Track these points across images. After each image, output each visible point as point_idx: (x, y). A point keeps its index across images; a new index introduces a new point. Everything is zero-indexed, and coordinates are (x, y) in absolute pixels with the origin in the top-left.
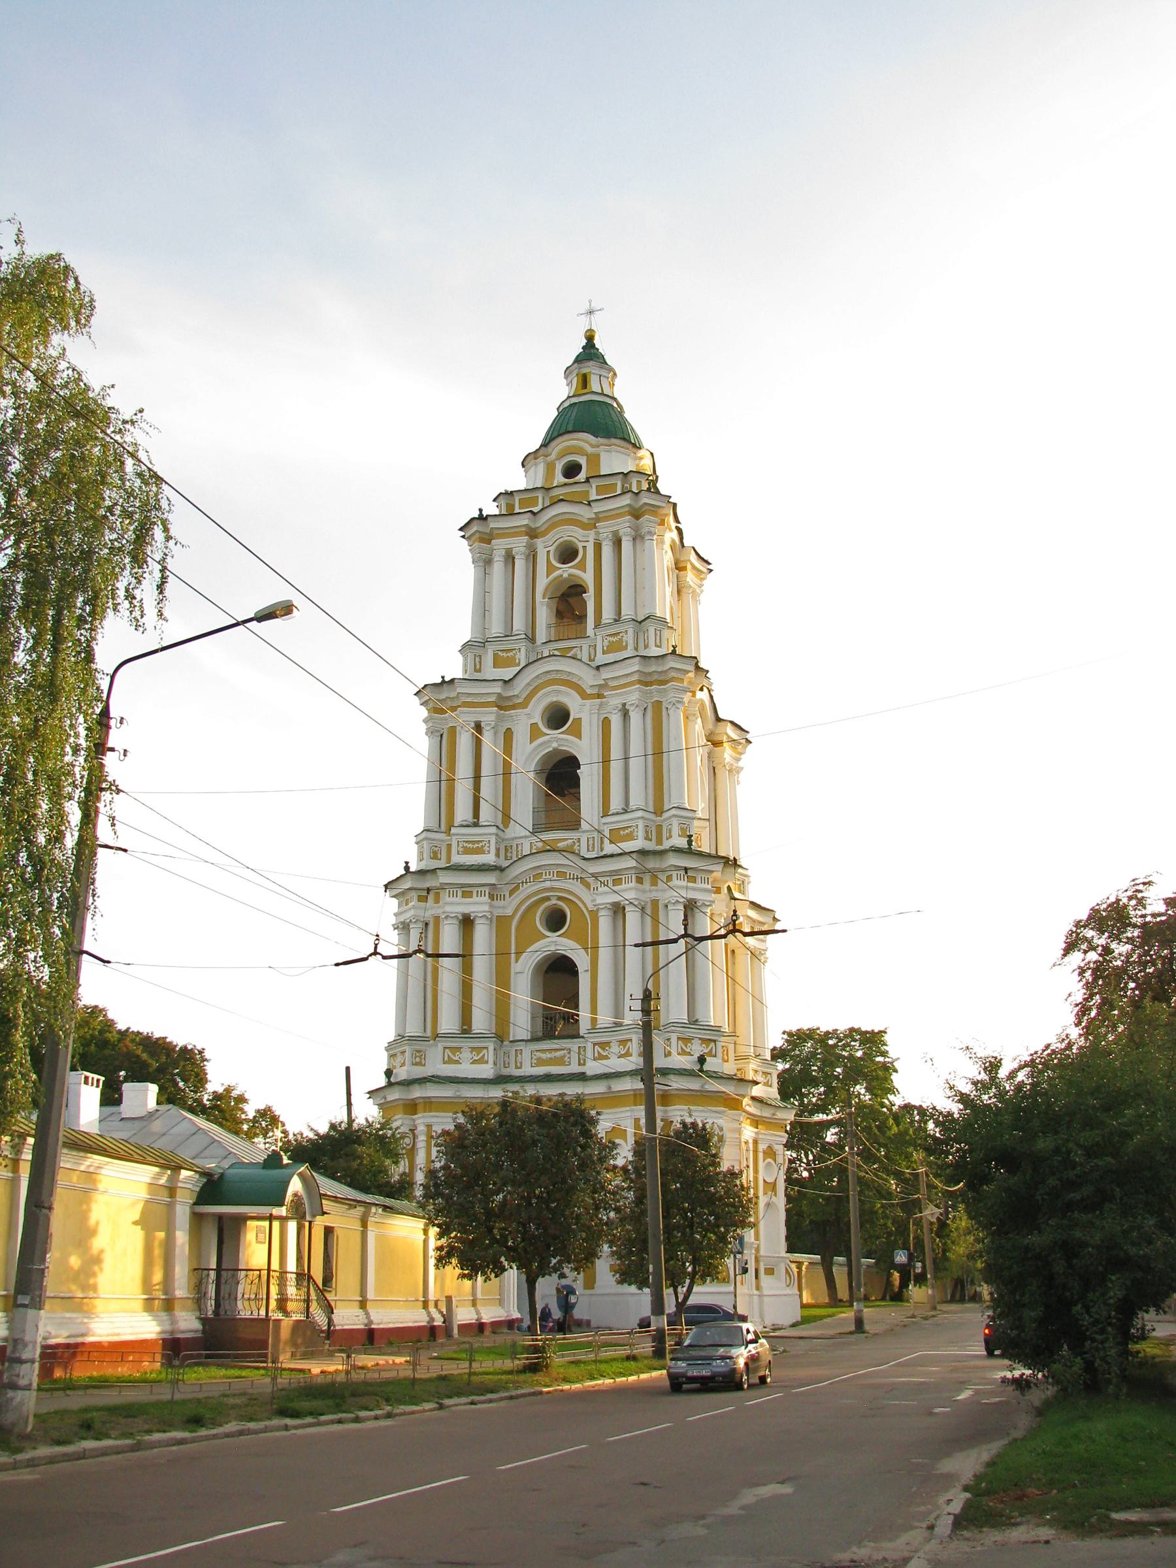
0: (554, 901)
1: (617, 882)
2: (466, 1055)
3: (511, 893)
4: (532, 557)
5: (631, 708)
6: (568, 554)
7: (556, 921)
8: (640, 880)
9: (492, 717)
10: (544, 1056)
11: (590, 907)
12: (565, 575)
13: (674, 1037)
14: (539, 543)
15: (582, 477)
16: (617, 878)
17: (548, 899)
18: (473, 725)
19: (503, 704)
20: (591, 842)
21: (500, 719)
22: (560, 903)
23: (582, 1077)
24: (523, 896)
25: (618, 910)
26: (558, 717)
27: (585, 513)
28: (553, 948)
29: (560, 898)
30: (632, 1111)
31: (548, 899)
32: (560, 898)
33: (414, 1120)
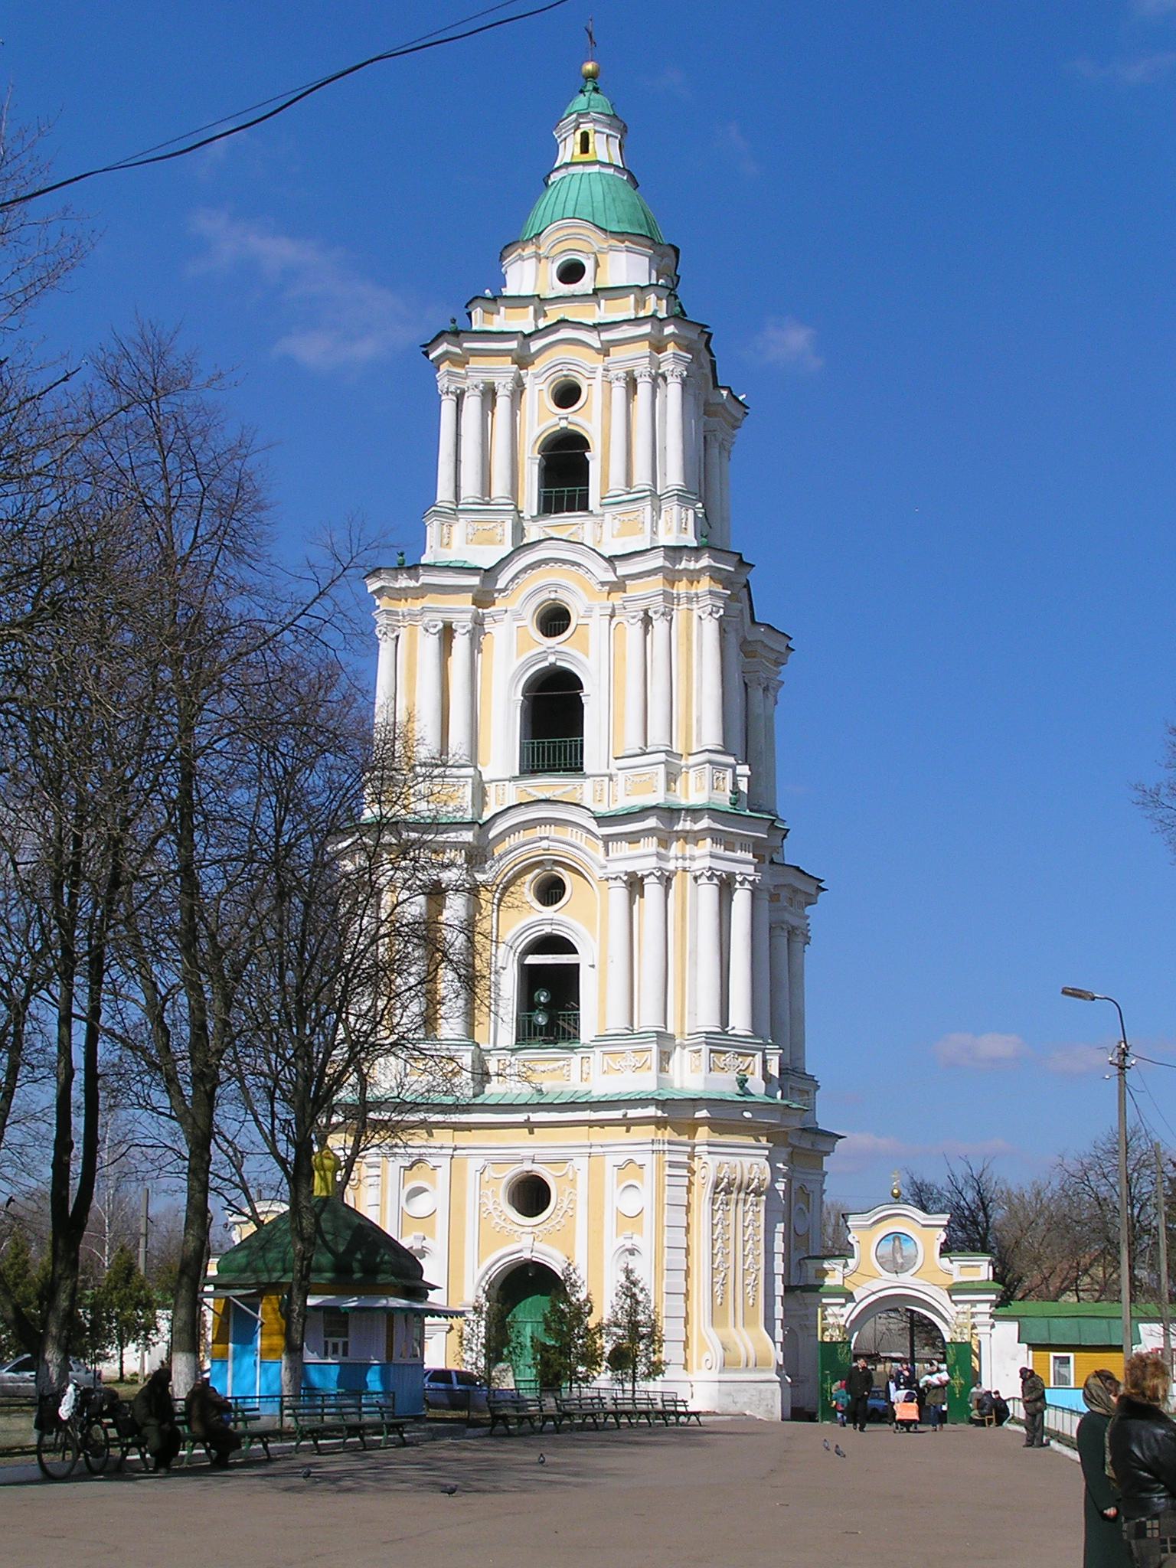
4: (518, 390)
5: (654, 617)
6: (567, 395)
7: (551, 891)
8: (664, 843)
9: (469, 616)
11: (599, 873)
12: (564, 424)
13: (705, 1049)
14: (529, 376)
15: (585, 285)
16: (633, 838)
18: (441, 625)
19: (483, 598)
20: (598, 788)
21: (478, 622)
25: (635, 884)
26: (554, 620)
27: (592, 338)
28: (548, 929)
31: (539, 864)
32: (556, 863)
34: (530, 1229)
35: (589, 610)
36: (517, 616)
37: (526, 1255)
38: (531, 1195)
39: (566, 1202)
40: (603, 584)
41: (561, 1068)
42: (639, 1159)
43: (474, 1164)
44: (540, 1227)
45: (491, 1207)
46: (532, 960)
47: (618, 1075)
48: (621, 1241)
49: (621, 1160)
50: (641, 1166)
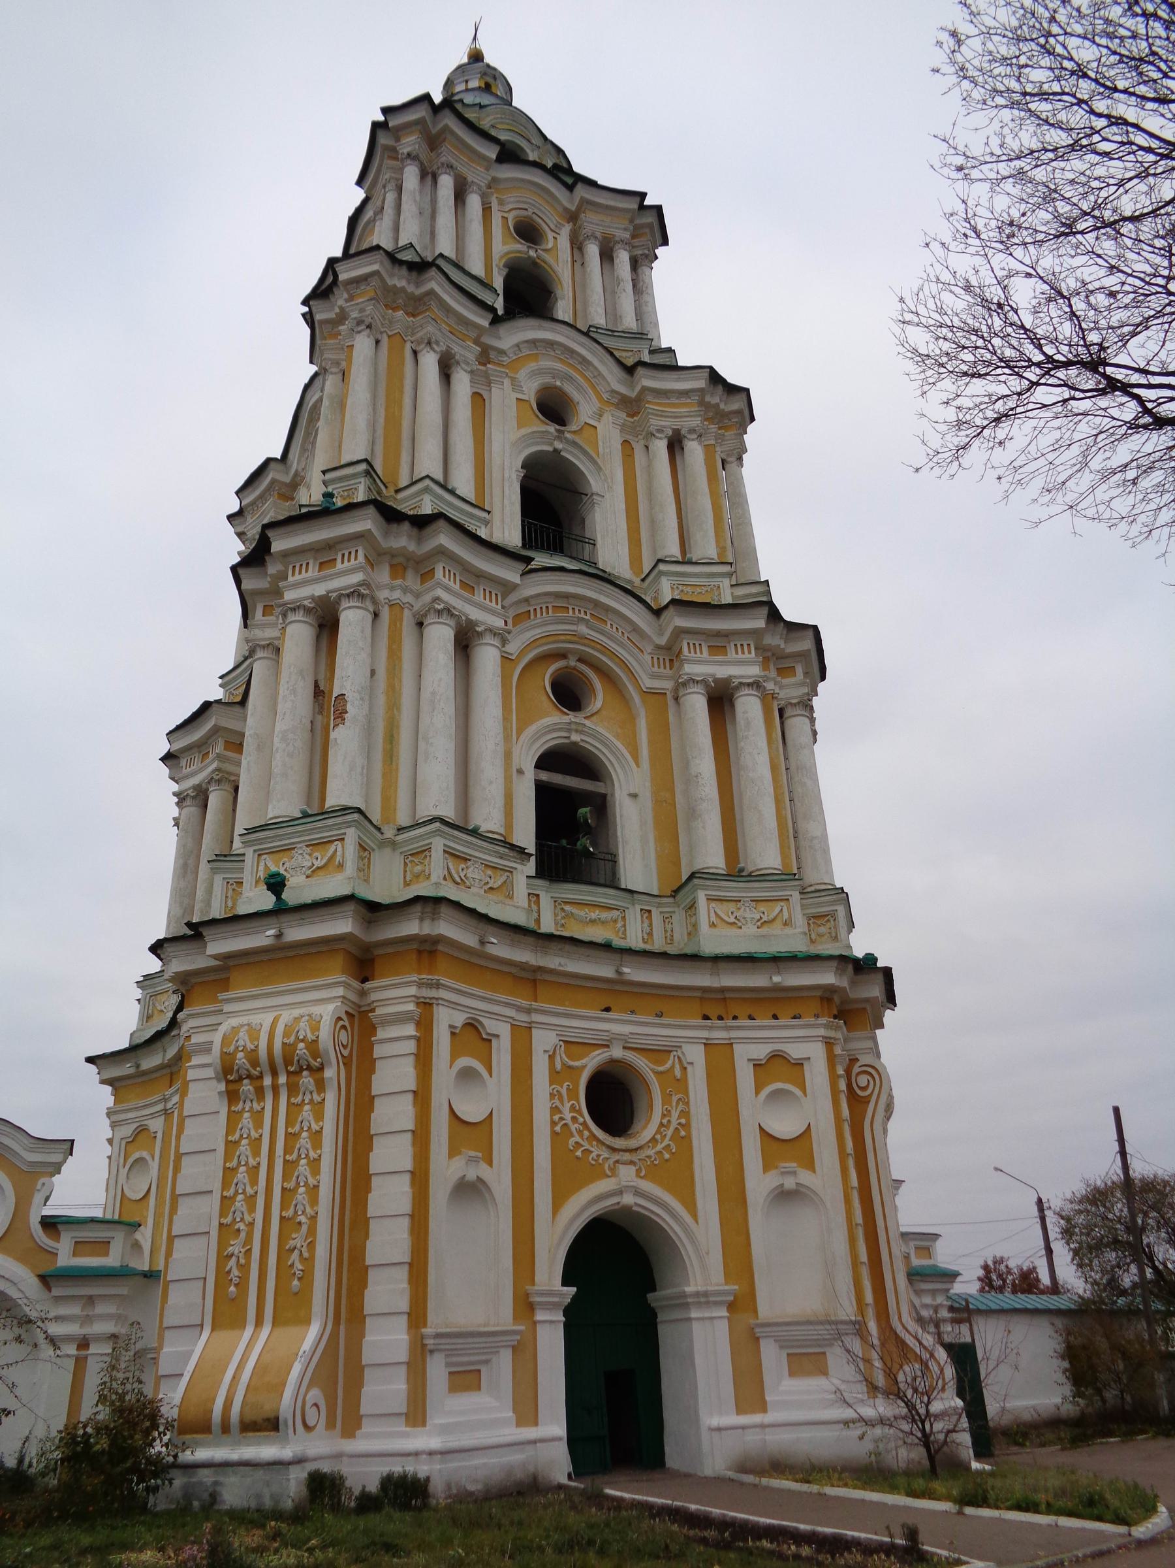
0: (572, 663)
1: (722, 650)
2: (474, 872)
3: (518, 619)
7: (568, 694)
10: (574, 911)
11: (648, 683)
16: (718, 643)
17: (563, 655)
22: (583, 667)
23: (694, 958)
24: (537, 633)
28: (575, 737)
29: (580, 660)
30: (827, 1026)
31: (563, 655)
33: (363, 994)
34: (627, 1157)
35: (600, 415)
36: (516, 386)
37: (628, 1199)
38: (612, 1100)
39: (675, 1115)
40: (613, 391)
41: (616, 921)
42: (795, 1051)
43: (543, 1041)
44: (642, 1154)
45: (568, 1116)
46: (545, 776)
47: (734, 931)
48: (772, 1180)
49: (762, 1052)
50: (799, 1064)
